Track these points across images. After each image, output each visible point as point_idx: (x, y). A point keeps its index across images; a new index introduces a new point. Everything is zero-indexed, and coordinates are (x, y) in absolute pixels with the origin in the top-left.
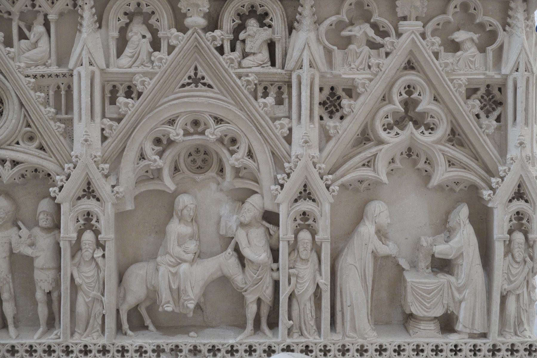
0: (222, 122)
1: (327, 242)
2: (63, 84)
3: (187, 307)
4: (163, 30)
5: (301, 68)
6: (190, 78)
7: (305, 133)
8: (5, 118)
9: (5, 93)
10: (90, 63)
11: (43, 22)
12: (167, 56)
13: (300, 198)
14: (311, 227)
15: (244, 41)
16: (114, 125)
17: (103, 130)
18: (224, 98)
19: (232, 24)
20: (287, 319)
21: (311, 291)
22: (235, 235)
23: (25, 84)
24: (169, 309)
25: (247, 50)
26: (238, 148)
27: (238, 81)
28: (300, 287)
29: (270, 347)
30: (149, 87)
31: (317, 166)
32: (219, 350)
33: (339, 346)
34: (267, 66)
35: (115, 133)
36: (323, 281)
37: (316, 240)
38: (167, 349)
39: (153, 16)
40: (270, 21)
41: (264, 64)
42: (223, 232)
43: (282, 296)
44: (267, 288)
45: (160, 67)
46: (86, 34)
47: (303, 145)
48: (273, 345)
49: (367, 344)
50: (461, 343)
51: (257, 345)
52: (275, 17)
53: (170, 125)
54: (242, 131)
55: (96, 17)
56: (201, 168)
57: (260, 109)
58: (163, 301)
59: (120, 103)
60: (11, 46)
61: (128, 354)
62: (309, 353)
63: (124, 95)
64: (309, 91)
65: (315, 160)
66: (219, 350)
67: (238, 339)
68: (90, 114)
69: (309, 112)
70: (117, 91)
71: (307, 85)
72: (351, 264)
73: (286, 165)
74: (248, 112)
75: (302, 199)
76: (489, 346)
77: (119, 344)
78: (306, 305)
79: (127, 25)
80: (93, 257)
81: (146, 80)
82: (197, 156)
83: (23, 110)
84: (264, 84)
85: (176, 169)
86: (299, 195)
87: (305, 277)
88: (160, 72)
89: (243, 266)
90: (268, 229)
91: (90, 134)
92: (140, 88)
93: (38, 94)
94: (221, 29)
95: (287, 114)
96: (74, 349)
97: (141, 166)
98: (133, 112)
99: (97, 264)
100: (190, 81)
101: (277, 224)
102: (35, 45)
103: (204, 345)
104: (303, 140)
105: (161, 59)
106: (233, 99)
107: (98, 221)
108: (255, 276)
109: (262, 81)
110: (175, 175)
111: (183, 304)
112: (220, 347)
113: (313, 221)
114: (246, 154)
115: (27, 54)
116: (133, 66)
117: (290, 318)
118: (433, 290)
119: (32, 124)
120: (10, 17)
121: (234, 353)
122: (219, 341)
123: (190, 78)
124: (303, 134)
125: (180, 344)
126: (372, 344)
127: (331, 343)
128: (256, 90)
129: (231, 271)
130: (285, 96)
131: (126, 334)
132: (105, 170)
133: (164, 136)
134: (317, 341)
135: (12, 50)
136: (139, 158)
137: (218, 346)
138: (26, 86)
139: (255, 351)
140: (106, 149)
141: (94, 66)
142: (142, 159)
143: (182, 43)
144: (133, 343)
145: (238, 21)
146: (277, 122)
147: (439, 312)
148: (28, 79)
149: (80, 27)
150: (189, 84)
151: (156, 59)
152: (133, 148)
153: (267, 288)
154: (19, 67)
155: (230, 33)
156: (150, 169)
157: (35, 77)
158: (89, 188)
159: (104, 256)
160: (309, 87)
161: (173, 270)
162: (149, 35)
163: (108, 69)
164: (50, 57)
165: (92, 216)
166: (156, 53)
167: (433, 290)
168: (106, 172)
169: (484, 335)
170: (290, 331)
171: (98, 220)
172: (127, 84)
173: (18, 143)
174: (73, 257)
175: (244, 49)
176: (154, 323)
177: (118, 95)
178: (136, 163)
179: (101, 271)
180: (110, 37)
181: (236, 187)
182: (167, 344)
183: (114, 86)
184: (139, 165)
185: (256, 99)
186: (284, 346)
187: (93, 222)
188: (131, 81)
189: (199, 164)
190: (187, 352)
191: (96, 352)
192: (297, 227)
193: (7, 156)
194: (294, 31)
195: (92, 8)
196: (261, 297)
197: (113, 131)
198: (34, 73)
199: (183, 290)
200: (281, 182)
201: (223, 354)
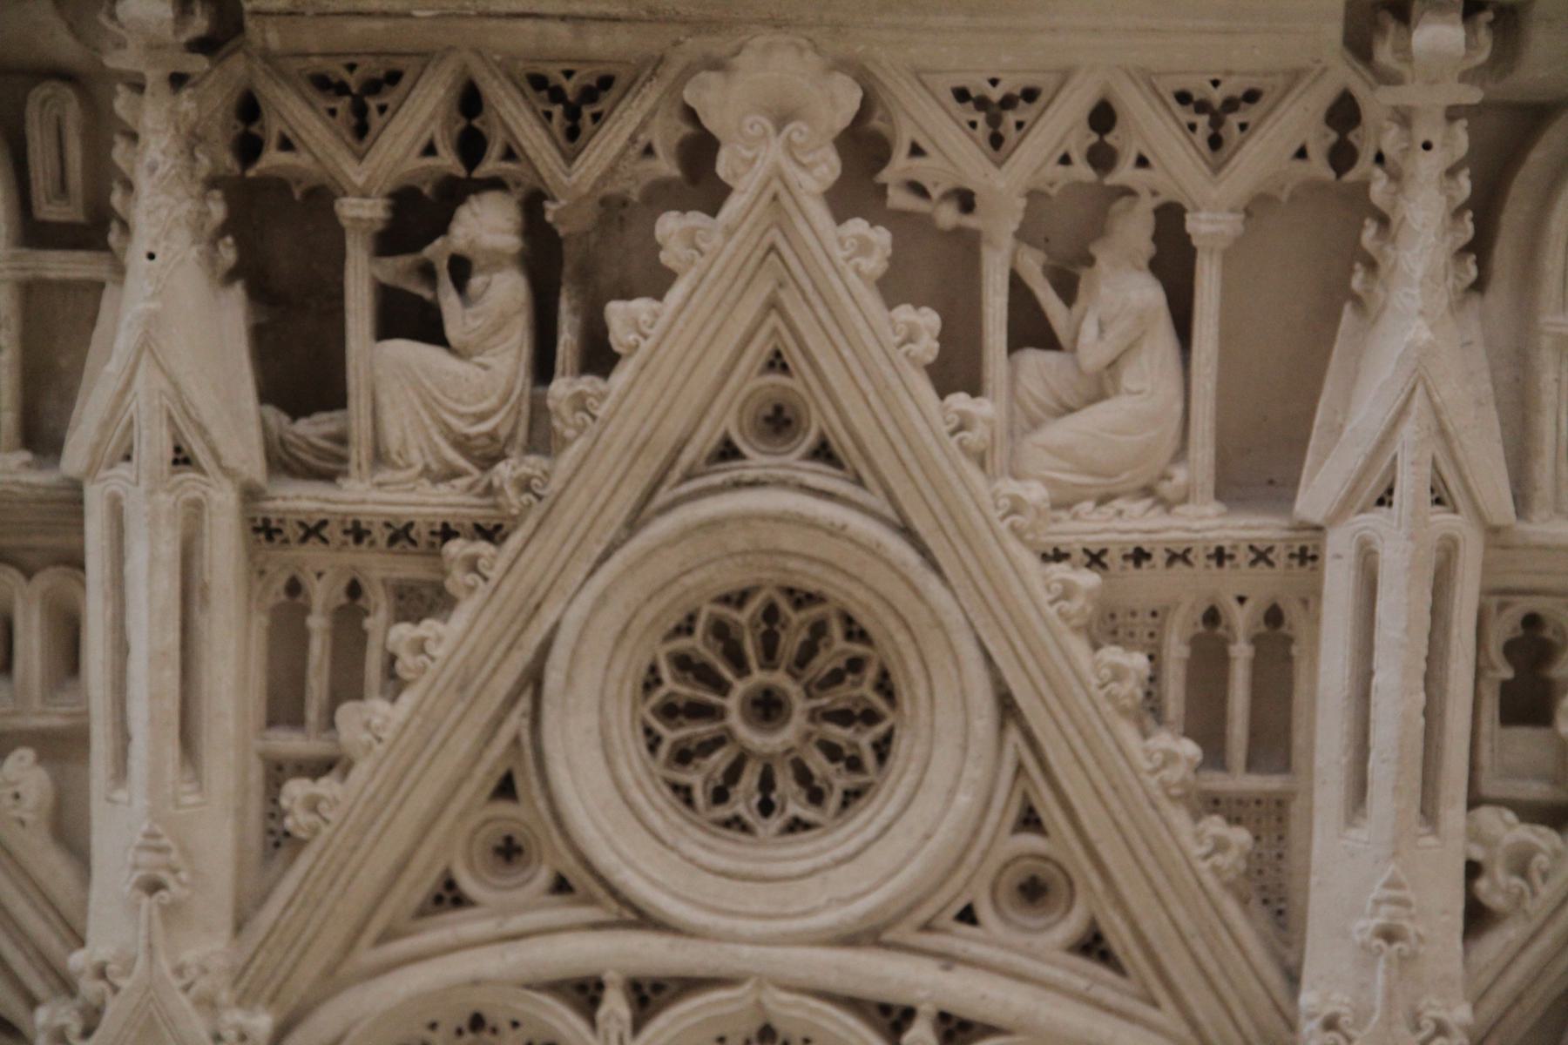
2: (1241, 600)
8: (910, 778)
9: (914, 640)
11: (1147, 248)
16: (1544, 845)
17: (1473, 870)
23: (1045, 598)
35: (1544, 891)
46: (1420, 322)
55: (1467, 229)
60: (975, 390)
68: (1417, 785)
83: (1014, 736)
91: (1413, 898)
93: (1113, 654)
102: (1101, 387)
115: (1060, 432)
119: (1050, 811)
120: (970, 221)
135: (982, 408)
138: (1051, 611)
140: (1485, 979)
141: (1455, 511)
148: (1059, 570)
149: (1365, 282)
154: (1016, 507)
157: (1095, 559)
163: (1523, 527)
164: (1181, 452)
173: (968, 916)
180: (1546, 342)
193: (921, 994)
195: (1451, 172)
197: (1537, 879)
198: (1094, 541)
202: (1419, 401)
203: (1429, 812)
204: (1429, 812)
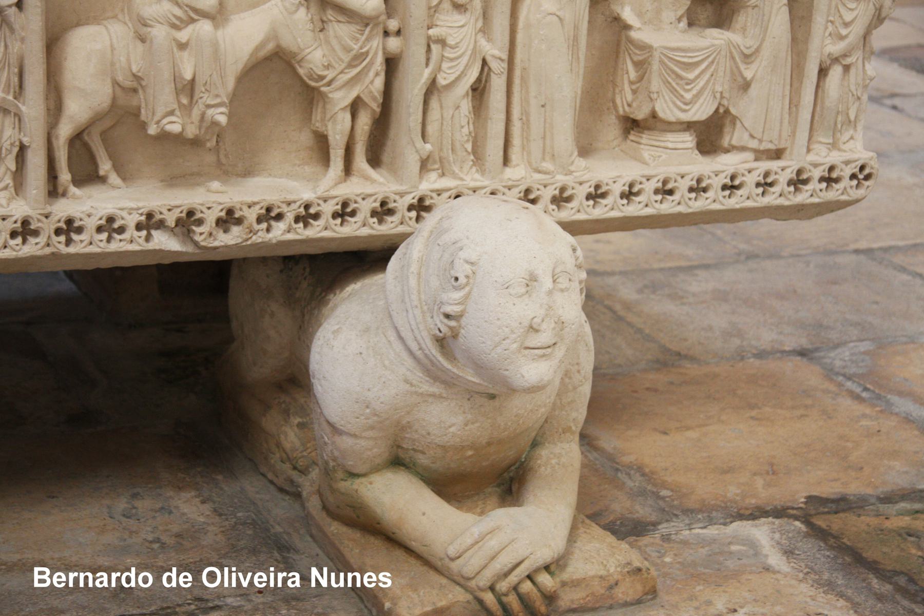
21: (473, 75)
28: (450, 68)
33: (520, 193)
36: (496, 52)
44: (377, 74)
49: (574, 185)
50: (743, 171)
51: (359, 199)
58: (160, 111)
61: (82, 237)
66: (279, 217)
72: (551, 14)
76: (789, 174)
77: (62, 215)
78: (458, 107)
87: (461, 45)
108: (356, 47)
111: (203, 116)
112: (284, 209)
118: (697, 64)
126: (581, 184)
127: (505, 187)
129: (299, 40)
134: (478, 184)
137: (279, 207)
139: (353, 213)
144: (94, 212)
147: (701, 111)
153: (377, 74)
161: (183, 35)
167: (697, 64)
169: (778, 154)
170: (425, 165)
186: (413, 198)
196: (362, 95)
201: (290, 225)
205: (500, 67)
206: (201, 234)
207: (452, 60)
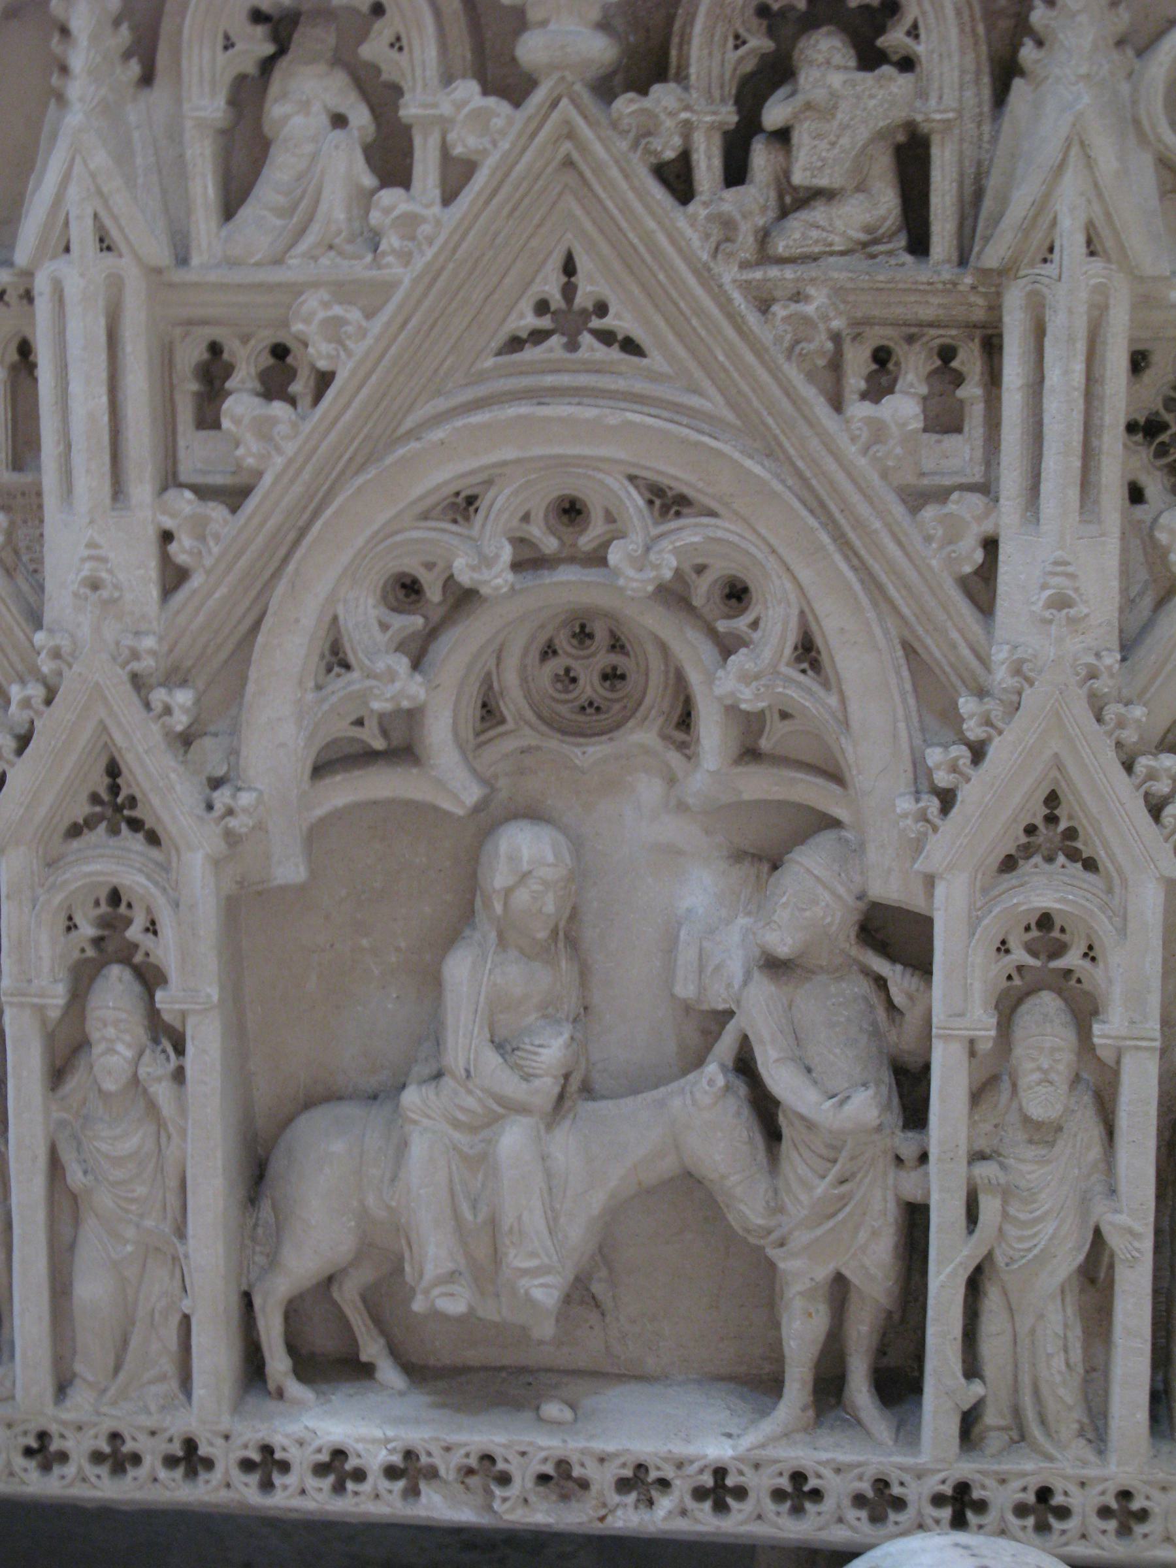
0: (685, 511)
1: (1146, 1049)
3: (529, 1299)
4: (419, 89)
5: (1045, 261)
6: (542, 307)
7: (1056, 563)
10: (101, 240)
12: (436, 209)
13: (1027, 851)
14: (1073, 982)
15: (783, 136)
17: (167, 537)
18: (695, 401)
19: (732, 56)
20: (959, 1374)
22: (738, 1002)
24: (455, 1304)
25: (798, 178)
26: (755, 625)
27: (752, 318)
28: (1020, 1239)
29: (882, 1484)
30: (359, 348)
31: (1112, 711)
32: (664, 1484)
34: (890, 253)
37: (1096, 1040)
38: (447, 1467)
39: (378, 25)
40: (909, 41)
41: (875, 241)
42: (685, 989)
43: (939, 1273)
44: (875, 1234)
45: (406, 258)
47: (1047, 614)
48: (894, 1477)
51: (827, 1472)
52: (932, 20)
53: (455, 521)
54: (774, 551)
55: (125, 34)
56: (598, 709)
57: (851, 451)
58: (431, 1271)
59: (237, 421)
62: (1052, 1520)
63: (258, 386)
64: (1079, 367)
65: (1103, 685)
66: (664, 1484)
67: (748, 1440)
69: (1077, 463)
70: (229, 370)
71: (1071, 340)
73: (967, 705)
74: (800, 464)
75: (1037, 859)
78: (1041, 1316)
79: (267, 65)
80: (135, 1080)
81: (349, 316)
82: (577, 658)
84: (877, 336)
85: (489, 712)
86: (1024, 839)
88: (407, 282)
89: (773, 1135)
90: (881, 983)
92: (320, 353)
94: (682, 78)
95: (976, 475)
96: (69, 1445)
97: (334, 699)
98: (290, 461)
99: (152, 1107)
100: (545, 322)
101: (922, 966)
103: (602, 1460)
104: (1048, 592)
105: (408, 223)
106: (732, 405)
107: (152, 928)
109: (868, 322)
110: (483, 738)
112: (669, 1473)
113: (1085, 955)
114: (788, 651)
116: (293, 252)
117: (972, 1369)
121: (730, 1501)
122: (665, 1449)
123: (542, 307)
124: (1049, 568)
125: (498, 1452)
128: (836, 365)
130: (972, 391)
131: (280, 1394)
132: (177, 713)
133: (430, 566)
136: (323, 664)
137: (658, 1469)
142: (337, 669)
143: (505, 145)
145: (759, 43)
146: (930, 512)
150: (538, 336)
151: (388, 221)
152: (297, 621)
153: (875, 1234)
155: (723, 100)
156: (372, 711)
158: (115, 789)
159: (179, 1075)
160: (1081, 346)
162: (360, 117)
165: (129, 906)
166: (390, 196)
168: (180, 721)
171: (153, 923)
172: (267, 337)
174: (57, 1075)
175: (787, 173)
176: (395, 1352)
177: (229, 385)
178: (311, 684)
179: (169, 1137)
180: (189, 124)
181: (746, 797)
182: (448, 1449)
183: (215, 349)
184: (324, 692)
185: (837, 404)
186: (943, 1482)
187: (134, 933)
188: (285, 324)
189: (589, 692)
190: (530, 1484)
191: (158, 1464)
192: (1010, 977)
194: (1018, 83)
199: (511, 1229)
200: (943, 779)
201: (682, 1500)
202: (78, 168)
203: (118, 490)
204: (118, 490)
205: (1130, 1247)
206: (505, 1500)
207: (1024, 1224)
